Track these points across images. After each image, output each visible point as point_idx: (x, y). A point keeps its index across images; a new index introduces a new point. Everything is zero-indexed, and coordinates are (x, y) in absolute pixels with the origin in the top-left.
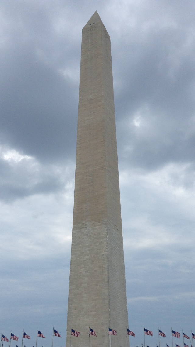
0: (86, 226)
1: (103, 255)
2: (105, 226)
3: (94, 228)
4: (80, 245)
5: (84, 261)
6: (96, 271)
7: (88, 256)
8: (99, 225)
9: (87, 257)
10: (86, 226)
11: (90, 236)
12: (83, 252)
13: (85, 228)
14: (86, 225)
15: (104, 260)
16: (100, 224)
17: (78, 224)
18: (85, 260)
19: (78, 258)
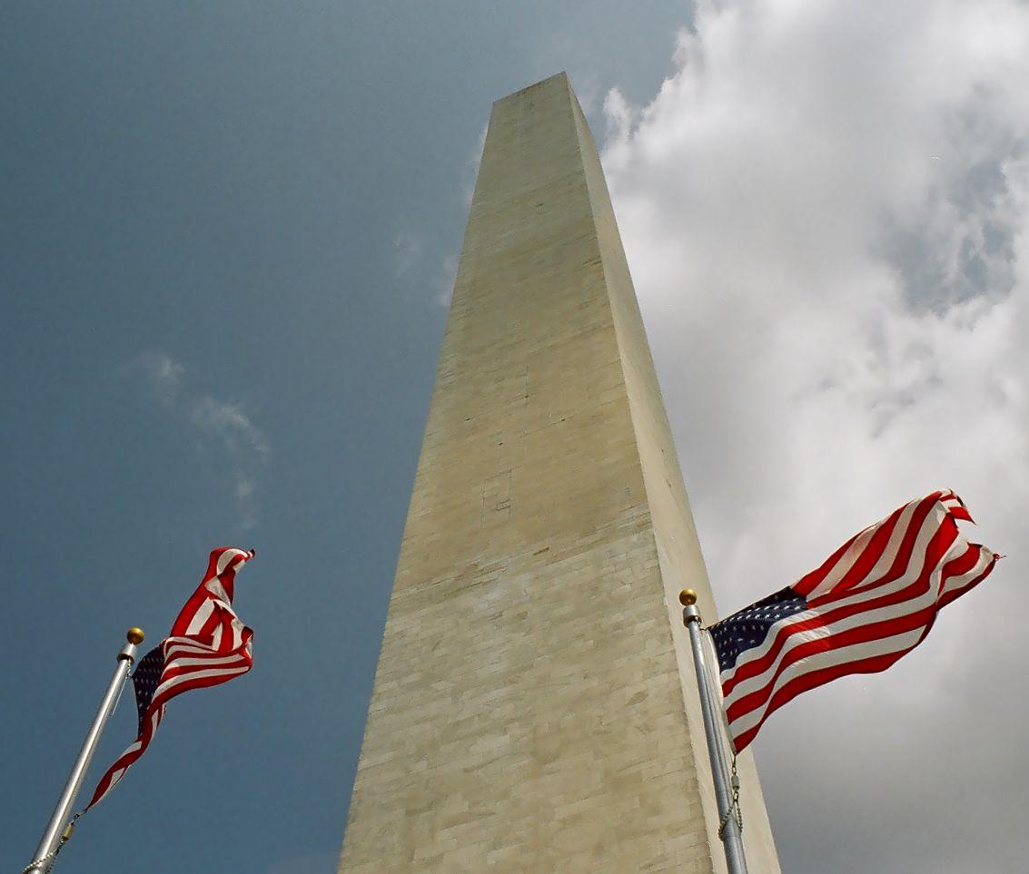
0: (485, 578)
1: (641, 696)
2: (634, 538)
3: (551, 567)
4: (441, 686)
5: (466, 771)
6: (576, 819)
7: (505, 732)
8: (590, 547)
9: (497, 743)
10: (485, 578)
11: (522, 616)
12: (461, 718)
13: (484, 584)
14: (491, 570)
15: (647, 729)
16: (598, 536)
17: (436, 580)
18: (480, 767)
19: (421, 766)
